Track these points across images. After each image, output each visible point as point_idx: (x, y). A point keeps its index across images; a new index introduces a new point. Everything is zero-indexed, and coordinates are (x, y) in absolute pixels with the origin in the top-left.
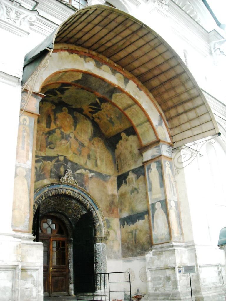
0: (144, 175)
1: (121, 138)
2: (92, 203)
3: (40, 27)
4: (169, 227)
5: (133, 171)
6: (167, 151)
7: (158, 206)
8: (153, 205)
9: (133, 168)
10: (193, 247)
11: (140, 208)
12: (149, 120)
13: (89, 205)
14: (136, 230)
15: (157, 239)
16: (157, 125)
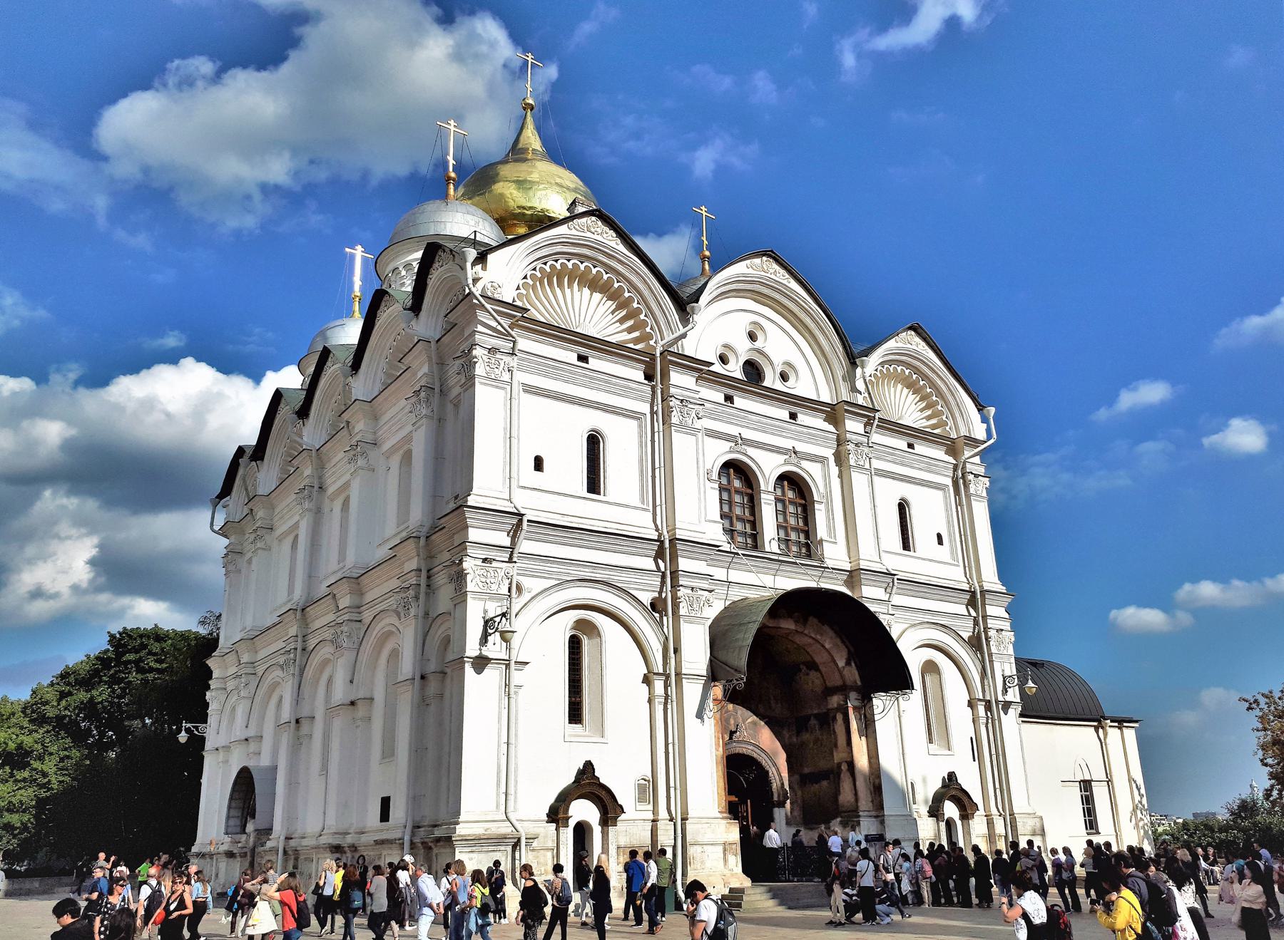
0: (829, 724)
1: (800, 670)
2: (767, 759)
3: (694, 531)
4: (856, 794)
5: (816, 716)
6: (856, 699)
7: (844, 767)
8: (839, 765)
9: (815, 712)
10: (882, 818)
11: (823, 765)
12: (834, 661)
13: (764, 762)
14: (820, 792)
15: (843, 806)
16: (844, 665)
